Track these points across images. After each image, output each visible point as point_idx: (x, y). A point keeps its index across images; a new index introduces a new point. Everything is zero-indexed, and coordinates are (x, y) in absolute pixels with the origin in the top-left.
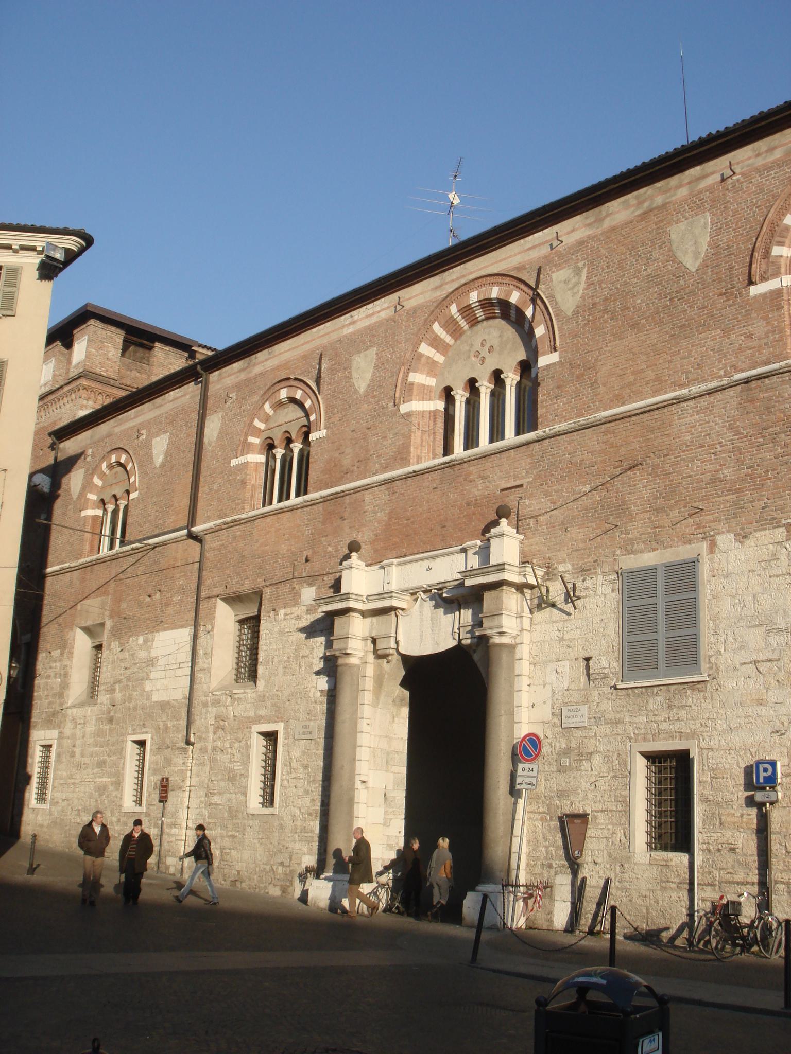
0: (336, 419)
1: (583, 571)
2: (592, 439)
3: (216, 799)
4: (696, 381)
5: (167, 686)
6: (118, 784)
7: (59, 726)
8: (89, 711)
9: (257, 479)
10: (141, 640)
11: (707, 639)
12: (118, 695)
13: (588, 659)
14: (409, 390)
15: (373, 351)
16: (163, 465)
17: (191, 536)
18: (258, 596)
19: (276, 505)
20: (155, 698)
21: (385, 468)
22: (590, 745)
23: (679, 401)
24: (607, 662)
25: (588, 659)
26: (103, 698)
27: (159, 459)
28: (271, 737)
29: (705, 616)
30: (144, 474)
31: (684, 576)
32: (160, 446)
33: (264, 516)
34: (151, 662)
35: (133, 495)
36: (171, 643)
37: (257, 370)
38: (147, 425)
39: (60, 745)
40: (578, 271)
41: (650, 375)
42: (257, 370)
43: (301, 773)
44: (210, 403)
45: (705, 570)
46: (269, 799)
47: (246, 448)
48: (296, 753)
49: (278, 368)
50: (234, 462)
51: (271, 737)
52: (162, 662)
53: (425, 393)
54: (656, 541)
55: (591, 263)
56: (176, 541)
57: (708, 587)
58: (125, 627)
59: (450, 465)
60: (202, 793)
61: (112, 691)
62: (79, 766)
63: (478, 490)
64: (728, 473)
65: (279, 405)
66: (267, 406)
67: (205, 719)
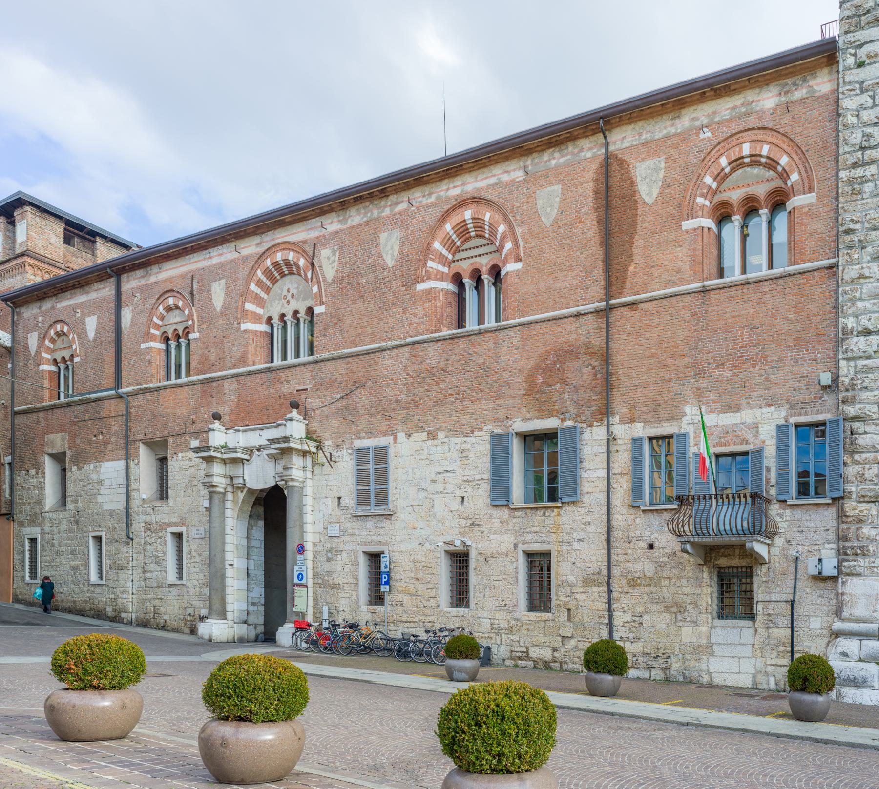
0: (204, 326)
1: (337, 447)
2: (341, 365)
3: (149, 575)
4: (389, 339)
5: (111, 500)
6: (87, 566)
7: (40, 525)
8: (60, 515)
9: (159, 360)
10: (92, 466)
11: (391, 491)
12: (80, 504)
13: (339, 498)
14: (246, 315)
15: (223, 282)
16: (95, 340)
17: (120, 397)
18: (164, 443)
19: (173, 381)
20: (105, 507)
21: (235, 366)
22: (341, 547)
23: (381, 350)
24: (349, 500)
25: (339, 498)
26: (70, 506)
27: (91, 334)
28: (179, 536)
29: (391, 477)
30: (82, 345)
31: (382, 454)
32: (91, 324)
33: (165, 388)
34: (100, 482)
35: (76, 359)
36: (111, 469)
37: (153, 279)
38: (80, 305)
39: (42, 538)
40: (334, 252)
41: (369, 330)
42: (153, 279)
43: (198, 559)
44: (123, 297)
45: (391, 452)
46: (180, 576)
47: (149, 337)
48: (194, 547)
49: (166, 281)
50: (143, 346)
51: (179, 536)
52: (107, 483)
53: (256, 318)
54: (370, 434)
55: (341, 248)
56: (109, 398)
57: (393, 462)
58: (80, 459)
59: (269, 370)
60: (140, 571)
61: (76, 502)
62: (58, 554)
63: (285, 389)
64: (403, 397)
65: (169, 309)
66: (161, 308)
67: (138, 525)
